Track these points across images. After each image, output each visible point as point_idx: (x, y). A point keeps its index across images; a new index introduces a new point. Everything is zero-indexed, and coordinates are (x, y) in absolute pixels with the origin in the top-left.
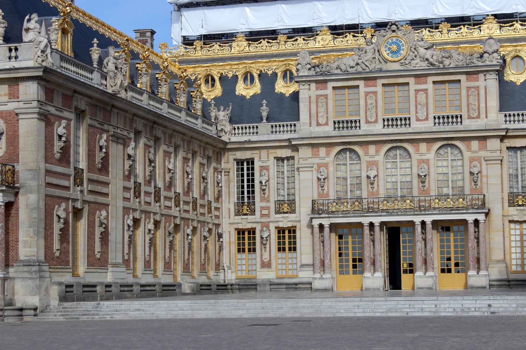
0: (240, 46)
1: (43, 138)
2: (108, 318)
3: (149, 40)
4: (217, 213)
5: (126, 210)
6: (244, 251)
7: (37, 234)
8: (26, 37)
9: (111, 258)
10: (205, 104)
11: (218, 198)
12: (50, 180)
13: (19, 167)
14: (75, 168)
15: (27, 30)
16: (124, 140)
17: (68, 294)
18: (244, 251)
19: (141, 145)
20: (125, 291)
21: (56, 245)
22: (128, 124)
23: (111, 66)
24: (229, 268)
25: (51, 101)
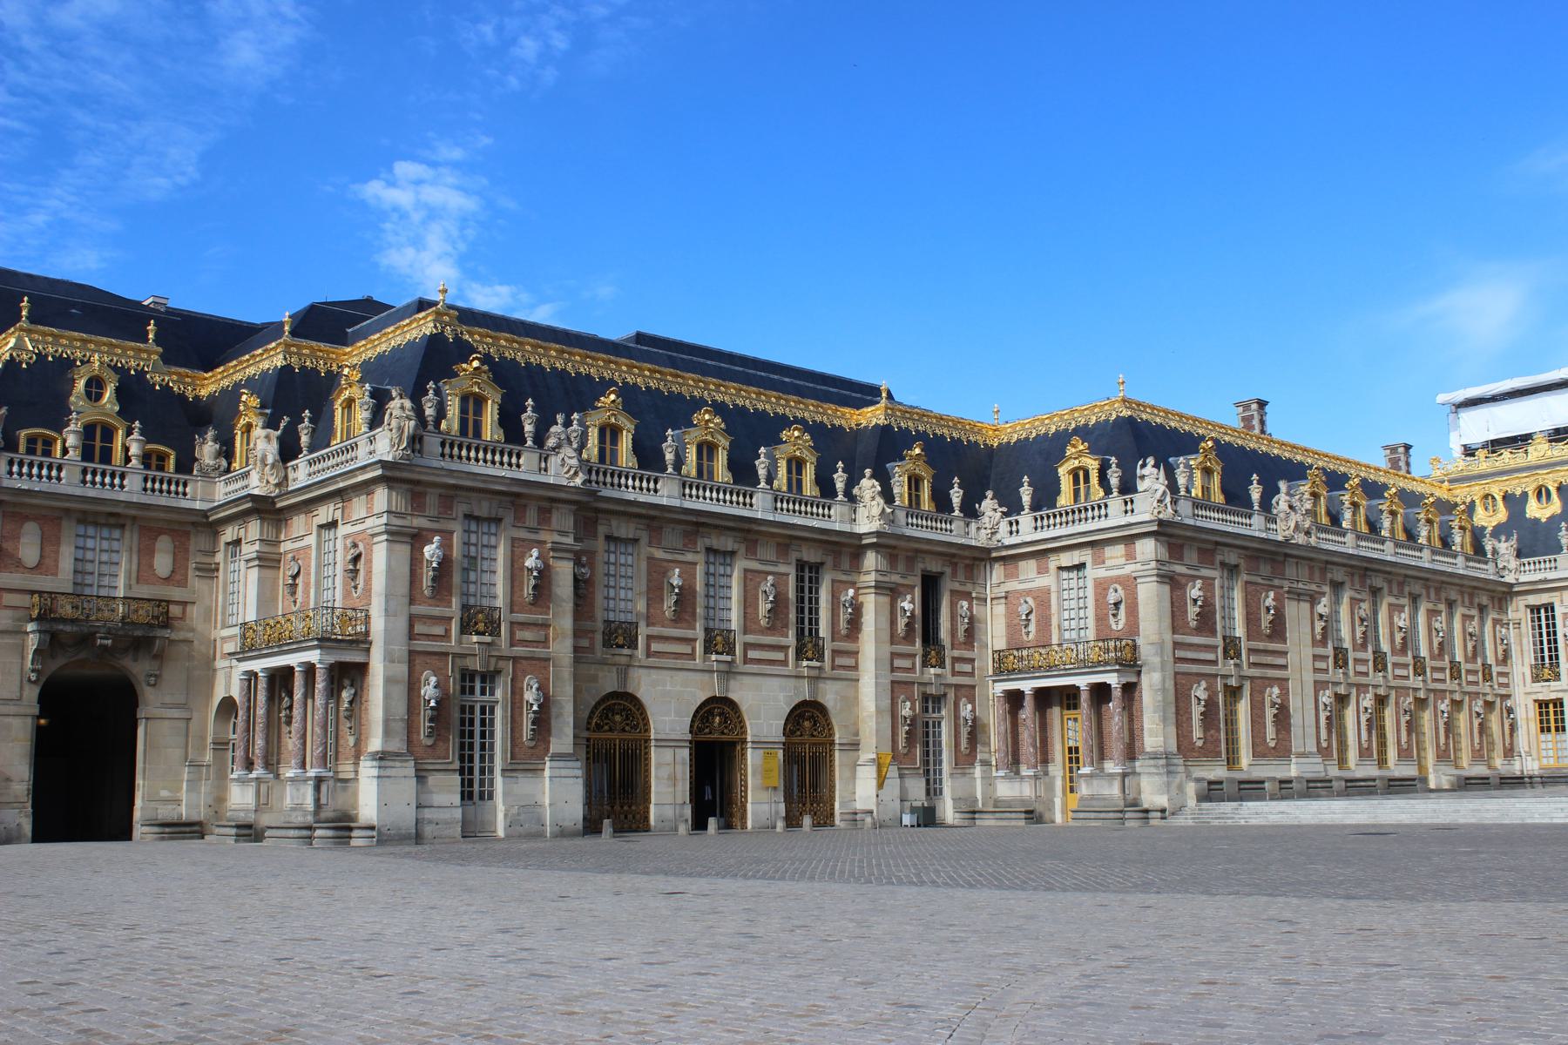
0: (1540, 451)
1: (1168, 604)
2: (1243, 822)
3: (1403, 458)
4: (1502, 680)
5: (1319, 686)
6: (1549, 730)
7: (1164, 720)
8: (1141, 486)
9: (1296, 745)
10: (1477, 535)
11: (1505, 658)
12: (1180, 654)
13: (1140, 641)
14: (1224, 638)
15: (1143, 477)
16: (1311, 596)
17: (1212, 792)
18: (1549, 730)
19: (1346, 600)
20: (1314, 788)
21: (1197, 733)
22: (1317, 574)
23: (1283, 506)
24: (1529, 754)
25: (1181, 558)
